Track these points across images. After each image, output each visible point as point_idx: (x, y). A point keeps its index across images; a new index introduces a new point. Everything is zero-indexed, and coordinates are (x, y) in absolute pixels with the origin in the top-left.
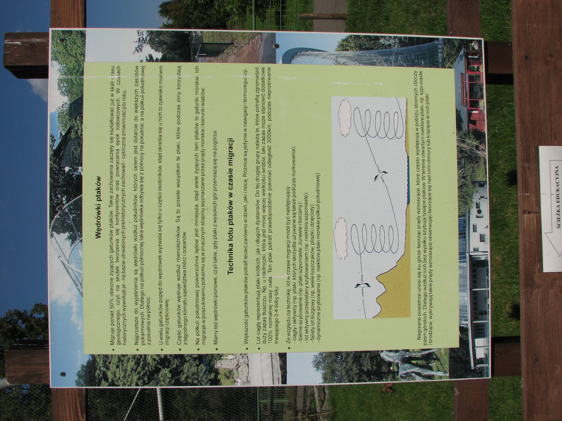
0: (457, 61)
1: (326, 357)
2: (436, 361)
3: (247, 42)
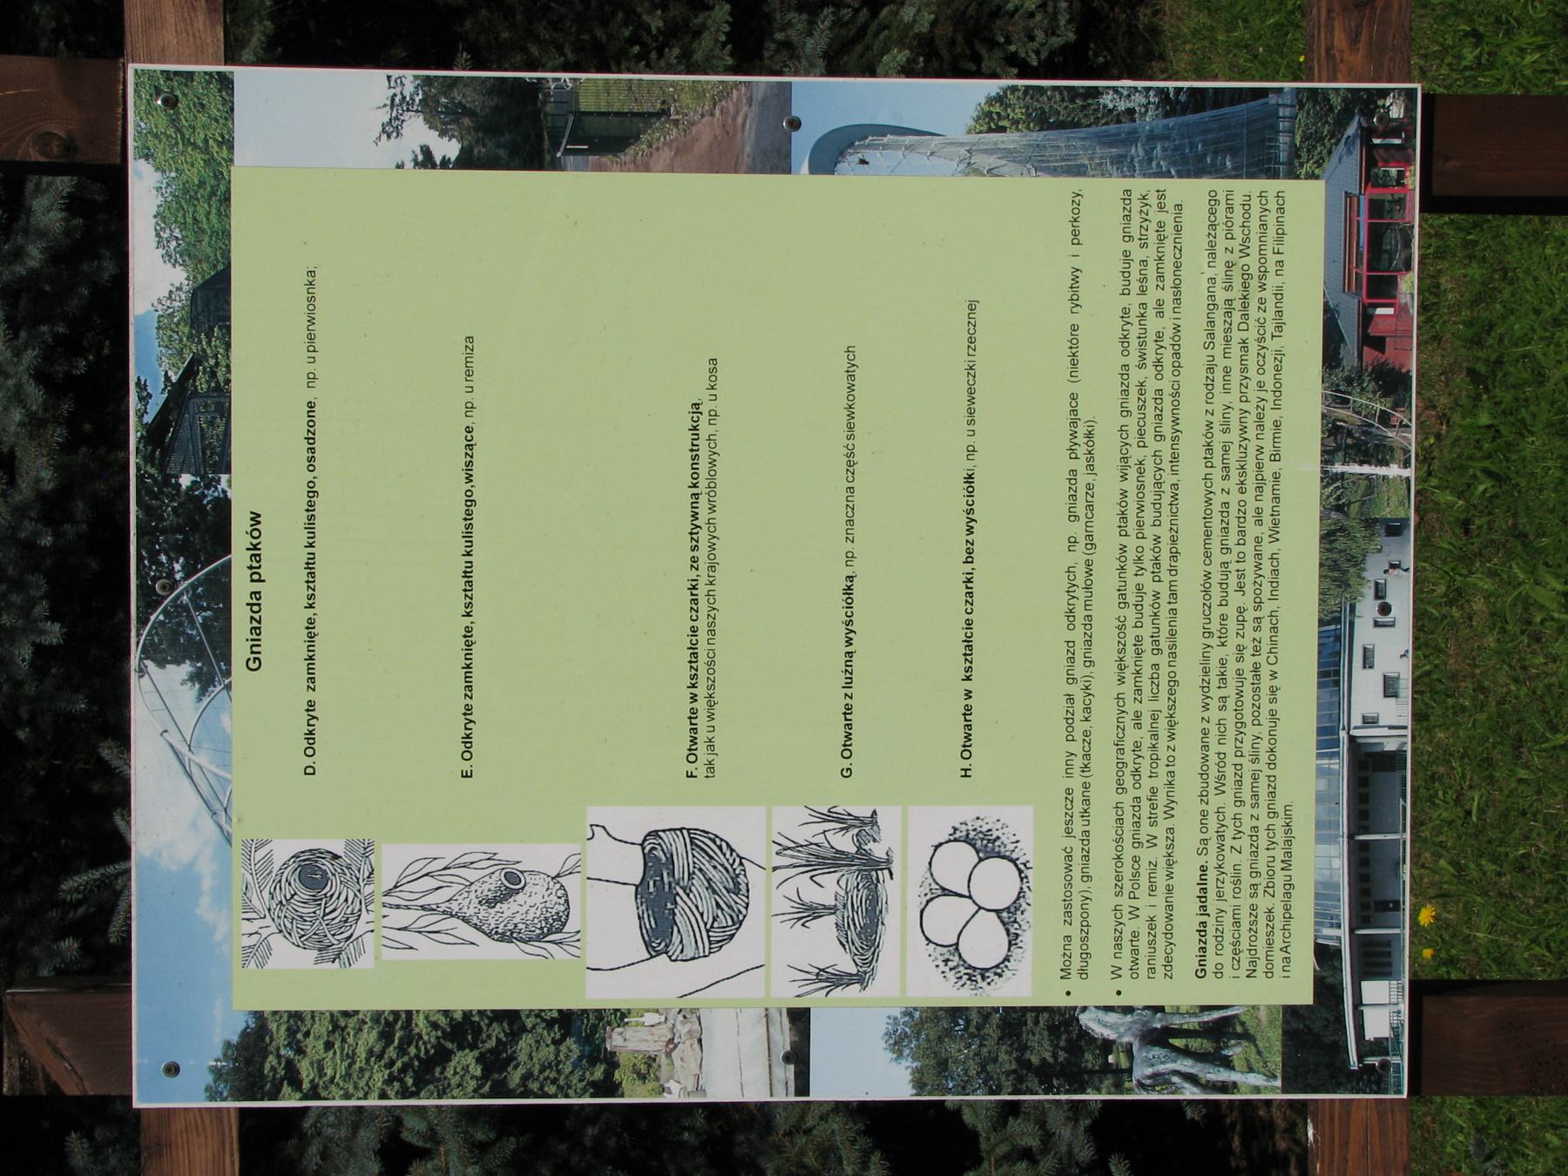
1: (922, 1022)
2: (1245, 1043)
3: (706, 108)
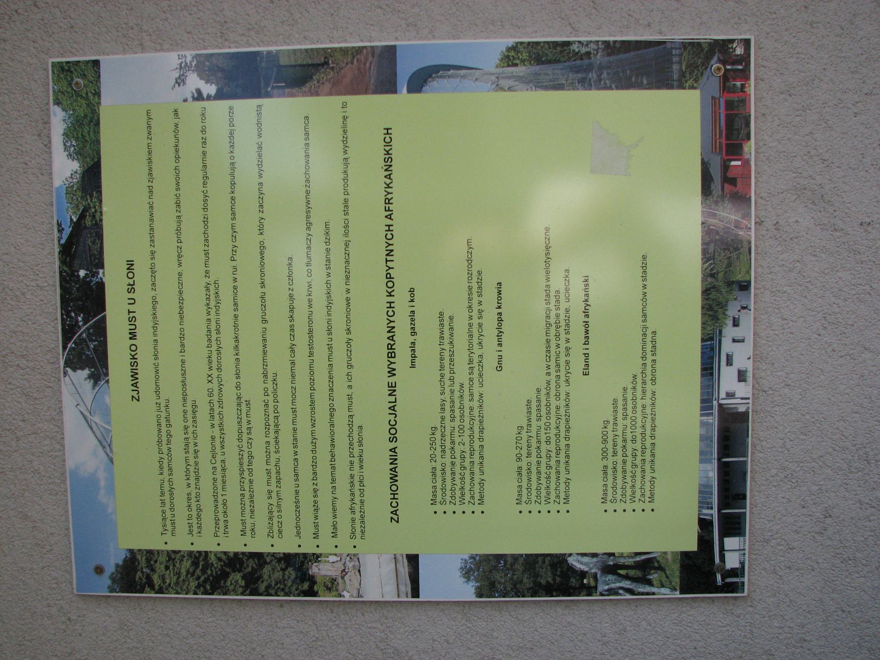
0: (705, 77)
2: (659, 572)
